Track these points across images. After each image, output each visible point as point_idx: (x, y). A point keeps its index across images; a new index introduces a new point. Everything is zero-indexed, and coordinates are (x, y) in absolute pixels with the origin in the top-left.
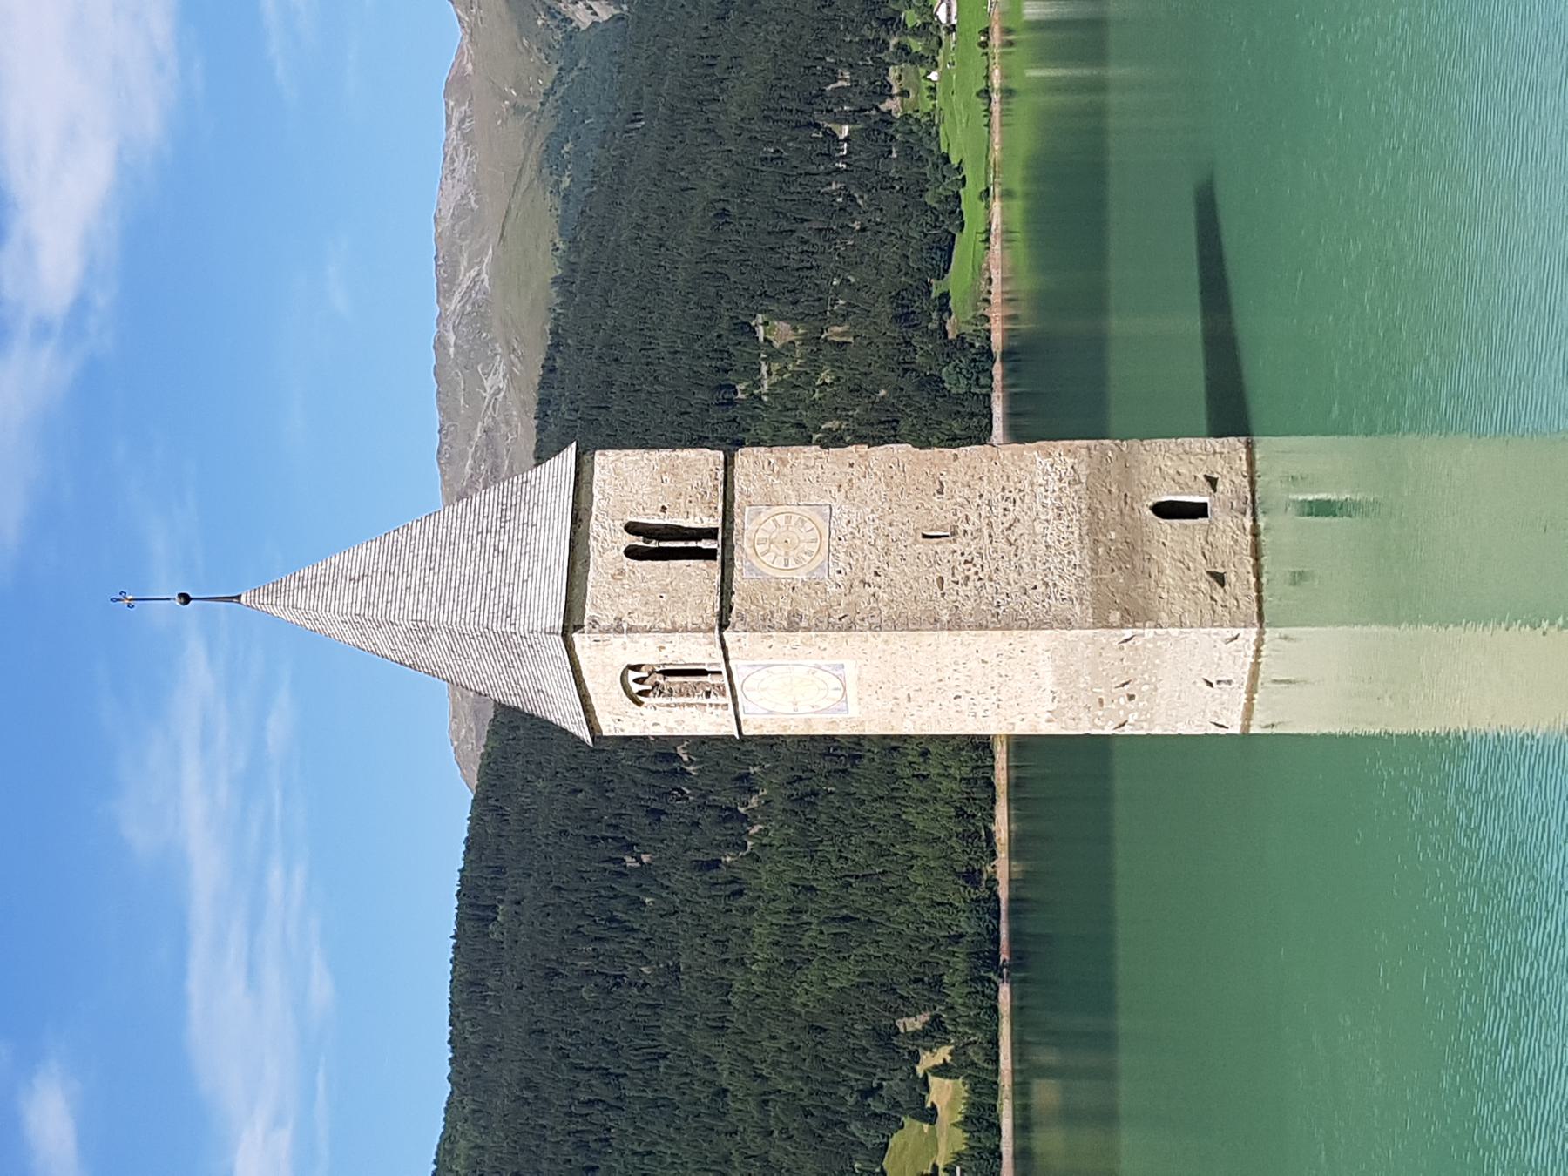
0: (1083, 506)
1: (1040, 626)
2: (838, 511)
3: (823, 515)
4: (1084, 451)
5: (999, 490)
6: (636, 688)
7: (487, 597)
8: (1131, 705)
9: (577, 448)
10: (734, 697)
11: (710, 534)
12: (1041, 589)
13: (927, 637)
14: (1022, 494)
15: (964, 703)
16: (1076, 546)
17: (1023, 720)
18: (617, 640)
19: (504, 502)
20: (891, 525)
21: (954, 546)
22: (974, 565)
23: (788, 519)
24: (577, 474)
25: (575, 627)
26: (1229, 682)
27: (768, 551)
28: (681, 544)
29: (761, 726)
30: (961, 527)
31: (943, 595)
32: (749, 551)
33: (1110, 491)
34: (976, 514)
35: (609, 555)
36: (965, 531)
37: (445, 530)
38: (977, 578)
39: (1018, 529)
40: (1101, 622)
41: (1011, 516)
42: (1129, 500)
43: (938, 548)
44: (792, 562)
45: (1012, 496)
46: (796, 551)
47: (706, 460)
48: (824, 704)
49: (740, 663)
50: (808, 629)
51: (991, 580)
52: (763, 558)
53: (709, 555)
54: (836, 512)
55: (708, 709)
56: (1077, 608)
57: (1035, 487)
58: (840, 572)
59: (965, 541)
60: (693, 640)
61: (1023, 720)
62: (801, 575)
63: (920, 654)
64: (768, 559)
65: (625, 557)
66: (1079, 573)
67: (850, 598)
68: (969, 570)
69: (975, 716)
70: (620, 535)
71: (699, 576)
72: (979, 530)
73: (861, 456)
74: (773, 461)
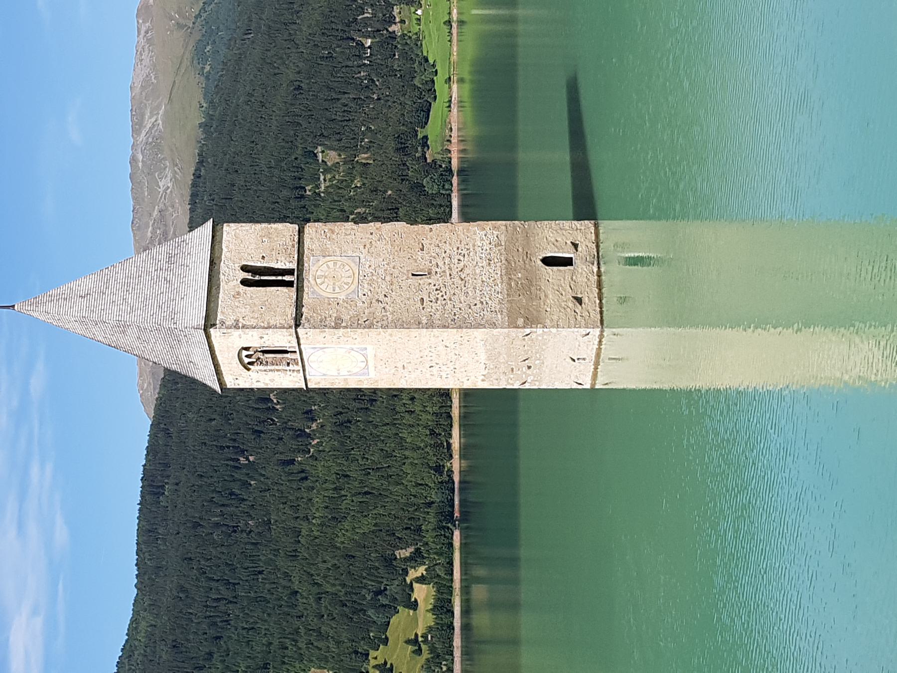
0: (503, 259)
1: (479, 326)
2: (364, 260)
3: (355, 262)
4: (504, 228)
5: (455, 249)
6: (247, 360)
8: (529, 372)
9: (213, 222)
10: (303, 366)
11: (290, 272)
12: (479, 305)
13: (414, 332)
14: (468, 251)
15: (435, 370)
16: (498, 282)
17: (468, 380)
18: (236, 333)
19: (171, 252)
20: (394, 268)
21: (430, 281)
22: (441, 292)
24: (213, 237)
25: (211, 325)
26: (584, 359)
27: (323, 283)
28: (273, 278)
29: (319, 383)
30: (434, 269)
31: (423, 308)
32: (312, 282)
33: (518, 250)
34: (443, 263)
35: (232, 284)
36: (436, 272)
37: (135, 269)
38: (443, 299)
39: (467, 271)
40: (513, 325)
41: (462, 264)
42: (528, 255)
43: (421, 282)
44: (337, 290)
45: (463, 252)
46: (340, 283)
47: (288, 230)
48: (355, 370)
49: (307, 346)
50: (346, 327)
51: (450, 300)
52: (320, 286)
53: (289, 284)
54: (362, 260)
55: (288, 372)
56: (499, 316)
58: (364, 295)
60: (280, 333)
61: (468, 380)
62: (342, 296)
63: (410, 342)
64: (323, 287)
65: (240, 285)
68: (438, 294)
69: (441, 378)
70: (238, 272)
71: (284, 296)
72: (444, 272)
73: (377, 229)
74: (326, 231)
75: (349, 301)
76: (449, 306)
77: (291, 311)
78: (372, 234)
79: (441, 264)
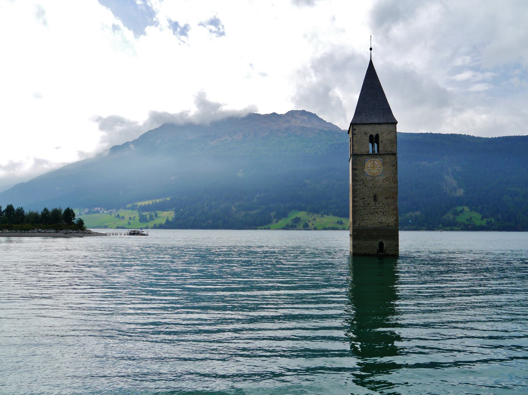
12: (362, 219)
16: (372, 226)
23: (379, 167)
27: (371, 163)
30: (377, 203)
32: (371, 160)
36: (376, 204)
39: (377, 215)
41: (379, 213)
43: (372, 198)
44: (368, 169)
45: (385, 214)
54: (381, 177)
56: (358, 226)
57: (387, 218)
62: (366, 170)
64: (370, 163)
66: (365, 227)
67: (360, 181)
72: (376, 206)
75: (364, 172)
76: (361, 208)
77: (359, 152)
78: (393, 180)
79: (380, 205)
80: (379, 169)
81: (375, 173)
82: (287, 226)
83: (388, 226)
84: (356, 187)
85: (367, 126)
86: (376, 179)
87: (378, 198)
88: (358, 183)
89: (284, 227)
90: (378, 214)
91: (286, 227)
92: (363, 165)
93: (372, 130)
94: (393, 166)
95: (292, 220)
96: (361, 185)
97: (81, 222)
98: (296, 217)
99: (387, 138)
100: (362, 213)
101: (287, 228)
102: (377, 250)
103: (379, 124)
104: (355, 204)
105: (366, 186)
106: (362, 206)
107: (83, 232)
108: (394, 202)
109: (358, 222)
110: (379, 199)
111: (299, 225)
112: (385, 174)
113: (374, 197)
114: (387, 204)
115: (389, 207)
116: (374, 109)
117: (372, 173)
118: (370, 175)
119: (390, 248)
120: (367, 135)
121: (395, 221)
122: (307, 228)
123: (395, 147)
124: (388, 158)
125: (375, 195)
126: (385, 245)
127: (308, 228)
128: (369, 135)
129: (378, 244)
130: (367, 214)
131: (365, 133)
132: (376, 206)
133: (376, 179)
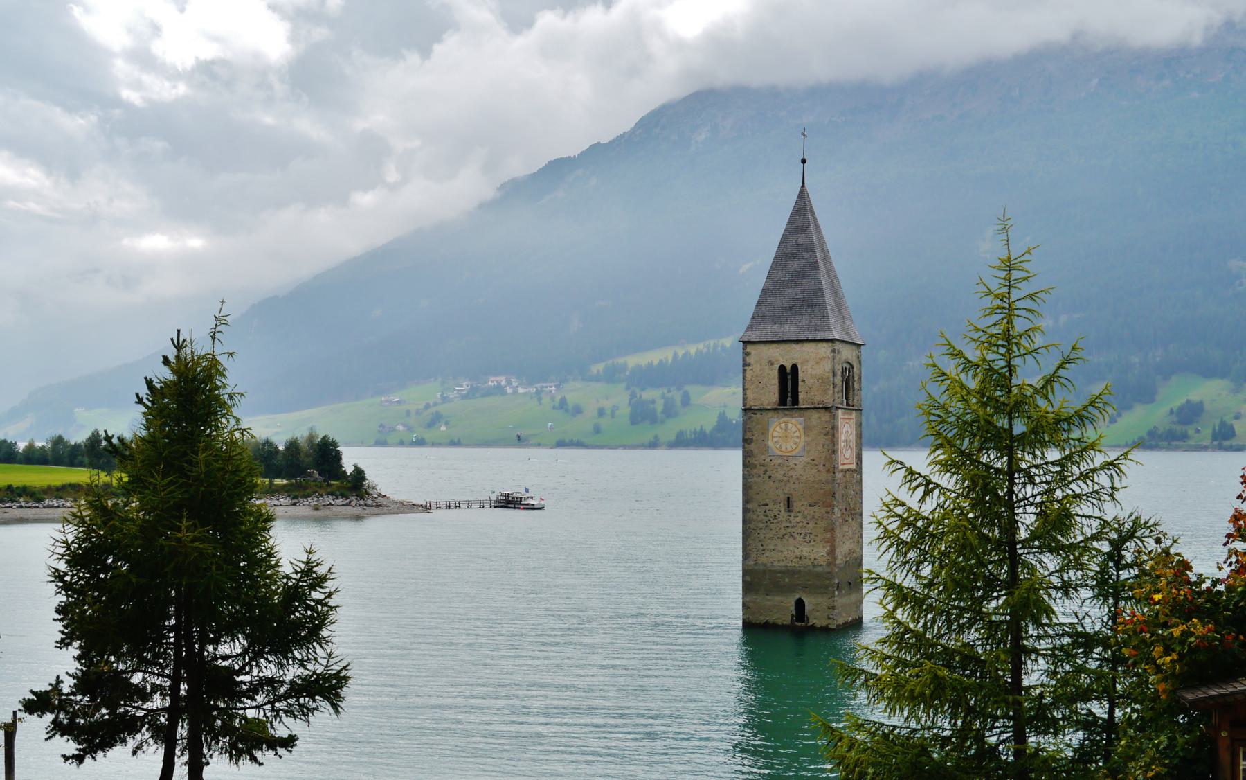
7: (770, 304)
11: (795, 401)
12: (762, 548)
16: (783, 564)
23: (798, 437)
27: (782, 429)
28: (789, 390)
30: (792, 514)
32: (782, 420)
39: (791, 540)
41: (797, 536)
43: (782, 504)
44: (775, 440)
53: (782, 401)
54: (801, 459)
59: (786, 516)
62: (770, 444)
64: (778, 429)
66: (769, 565)
72: (790, 522)
75: (767, 448)
76: (761, 525)
79: (798, 520)
80: (798, 440)
81: (790, 449)
82: (1152, 434)
83: (814, 566)
84: (750, 480)
85: (774, 346)
86: (791, 464)
87: (795, 504)
88: (755, 471)
89: (1141, 438)
90: (795, 538)
91: (1146, 437)
92: (765, 432)
93: (785, 356)
94: (826, 434)
95: (1172, 412)
96: (759, 476)
97: (359, 474)
98: (1188, 401)
99: (813, 373)
100: (762, 536)
101: (1153, 443)
102: (792, 616)
103: (797, 342)
104: (749, 515)
105: (770, 477)
106: (761, 521)
107: (362, 502)
108: (827, 513)
109: (753, 556)
110: (797, 505)
111: (1198, 431)
112: (808, 452)
113: (786, 503)
114: (813, 517)
115: (816, 524)
116: (794, 306)
117: (783, 449)
118: (780, 453)
119: (818, 614)
120: (773, 367)
121: (828, 554)
122: (1227, 443)
123: (831, 392)
124: (815, 415)
125: (789, 498)
126: (808, 607)
127: (1234, 442)
128: (777, 366)
129: (793, 603)
130: (771, 539)
131: (770, 361)
132: (790, 522)
133: (791, 464)
